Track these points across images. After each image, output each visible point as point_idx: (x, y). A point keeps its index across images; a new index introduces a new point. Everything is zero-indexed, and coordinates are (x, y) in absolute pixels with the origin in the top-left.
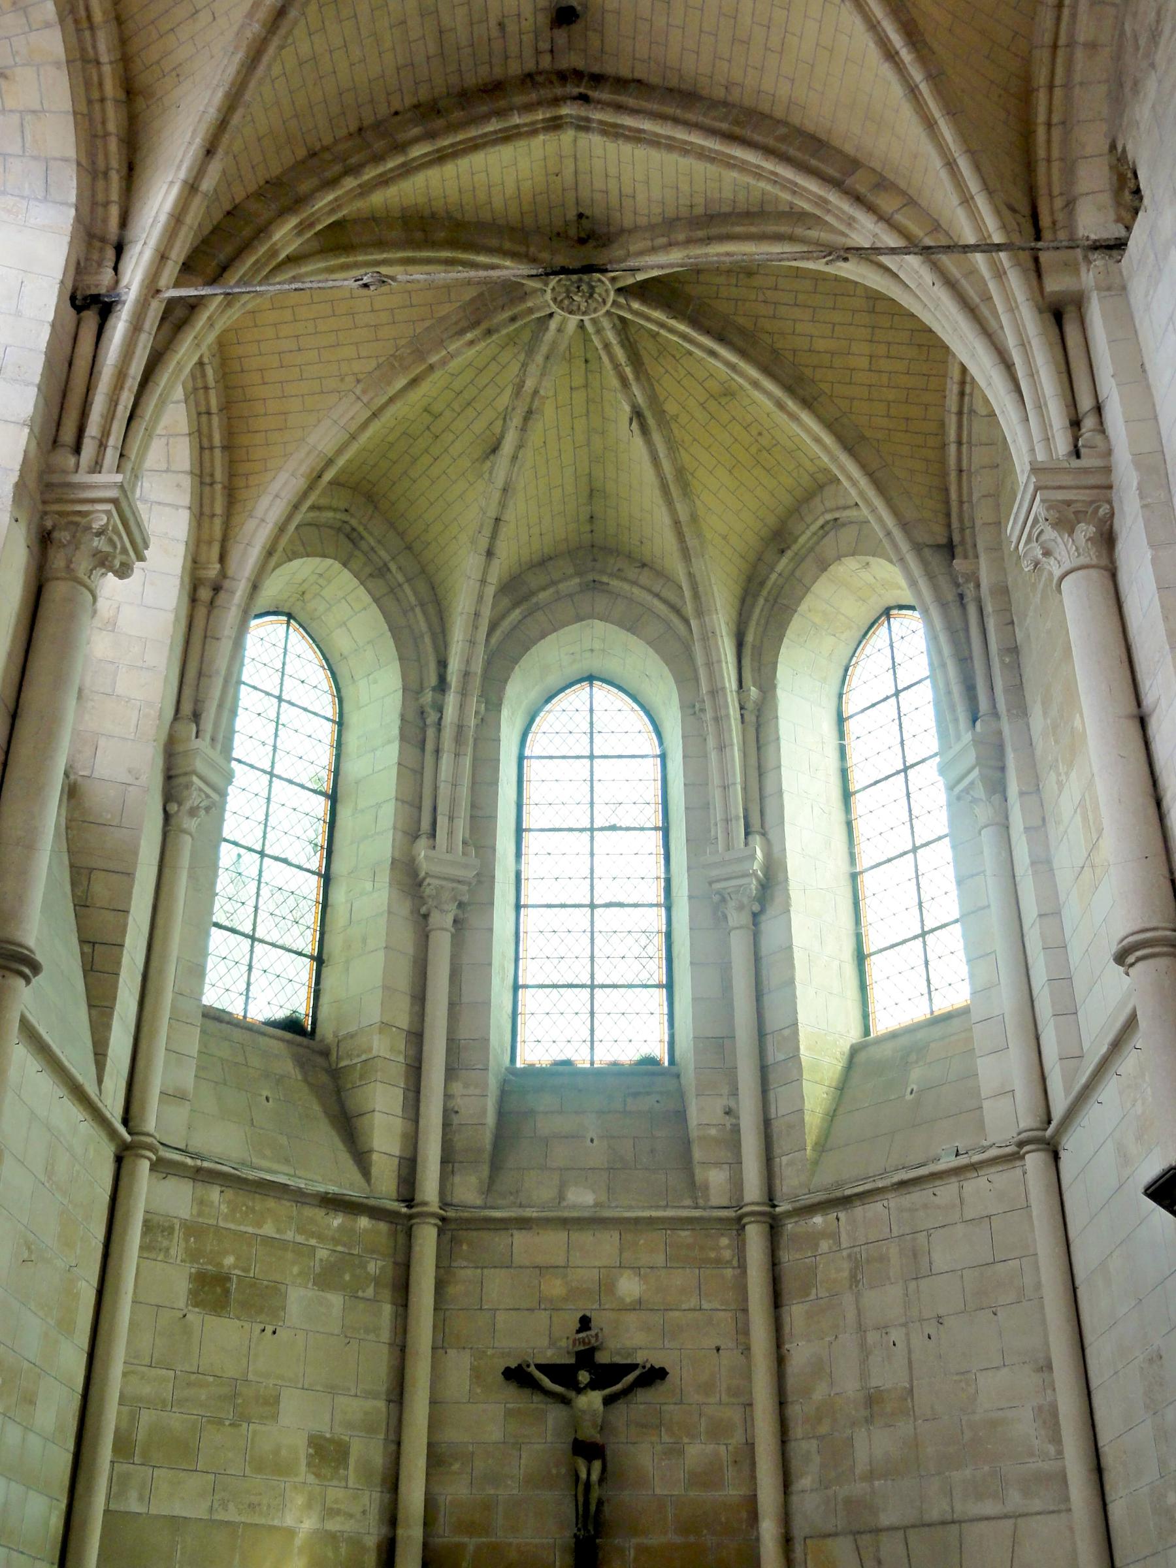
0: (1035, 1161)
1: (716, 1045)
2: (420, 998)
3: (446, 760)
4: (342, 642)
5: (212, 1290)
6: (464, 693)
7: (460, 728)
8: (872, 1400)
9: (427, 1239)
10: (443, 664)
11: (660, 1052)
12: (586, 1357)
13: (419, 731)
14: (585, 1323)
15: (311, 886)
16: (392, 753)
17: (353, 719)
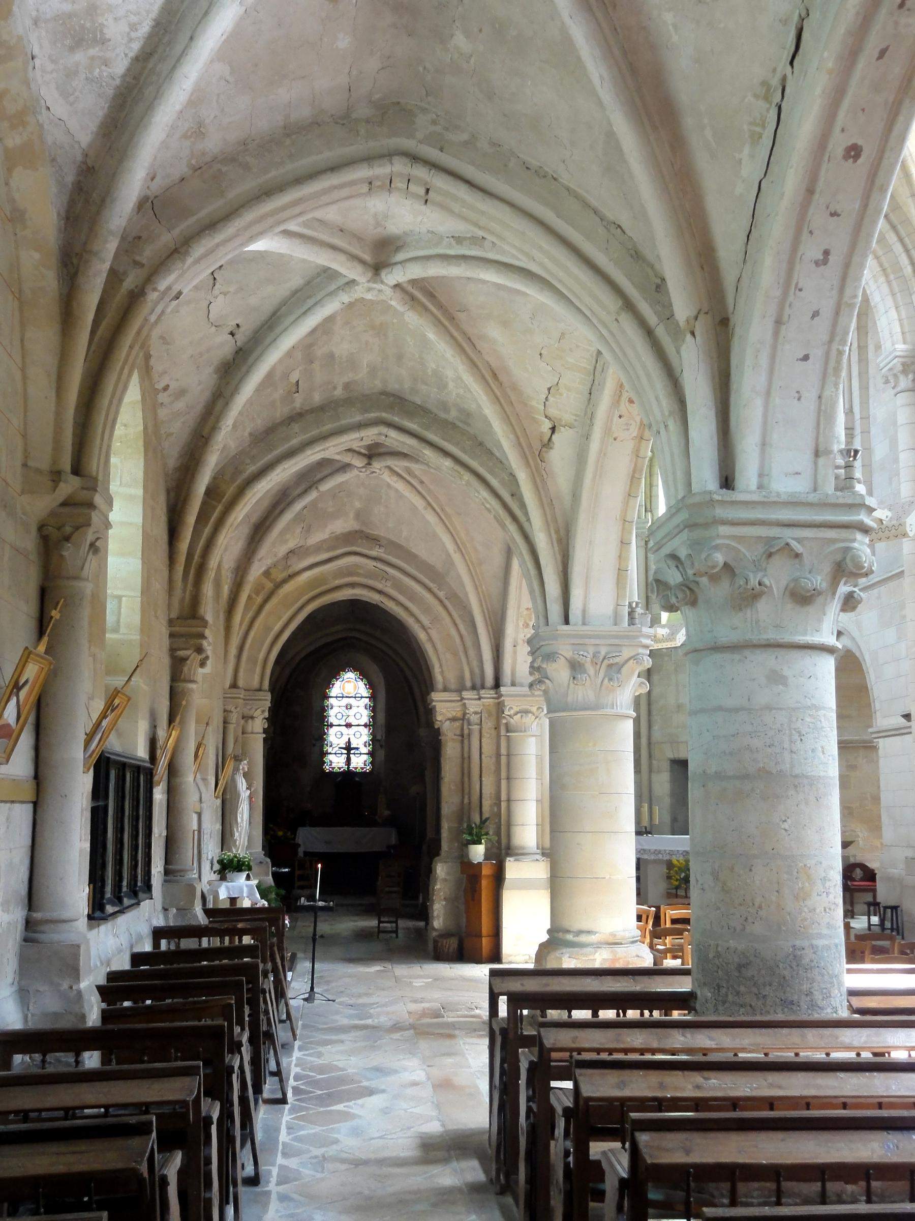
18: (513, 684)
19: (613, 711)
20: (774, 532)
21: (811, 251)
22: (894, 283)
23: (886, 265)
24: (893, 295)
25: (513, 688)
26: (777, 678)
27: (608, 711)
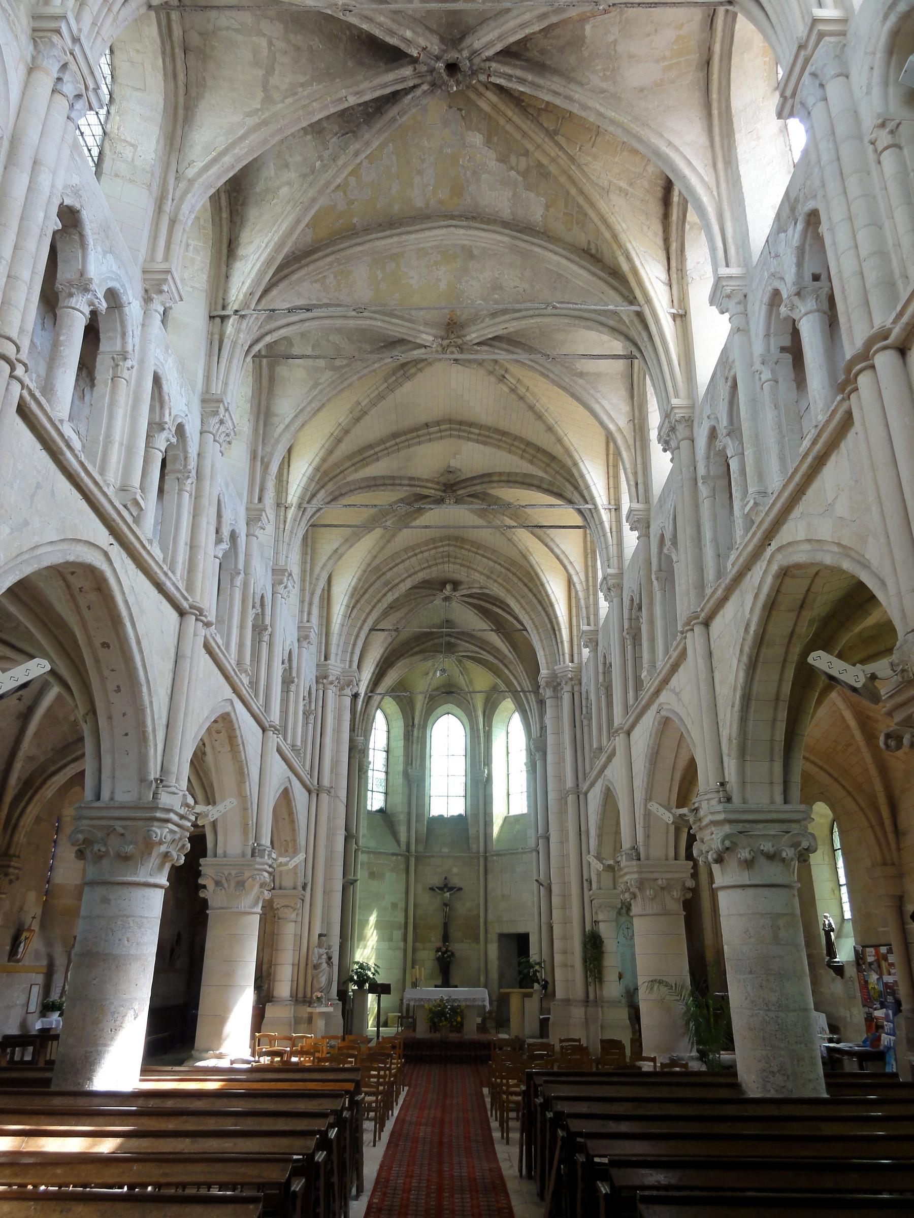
0: (534, 854)
1: (476, 816)
2: (410, 804)
3: (414, 746)
4: (388, 711)
5: (372, 875)
6: (419, 729)
7: (418, 738)
8: (503, 896)
9: (412, 861)
10: (413, 719)
11: (463, 812)
12: (446, 885)
13: (408, 736)
14: (446, 878)
15: (383, 776)
16: (401, 743)
17: (392, 731)
18: (280, 889)
19: (237, 910)
20: (112, 823)
21: (111, 687)
22: (542, 634)
23: (537, 624)
24: (541, 641)
25: (281, 891)
26: (106, 901)
27: (235, 910)
